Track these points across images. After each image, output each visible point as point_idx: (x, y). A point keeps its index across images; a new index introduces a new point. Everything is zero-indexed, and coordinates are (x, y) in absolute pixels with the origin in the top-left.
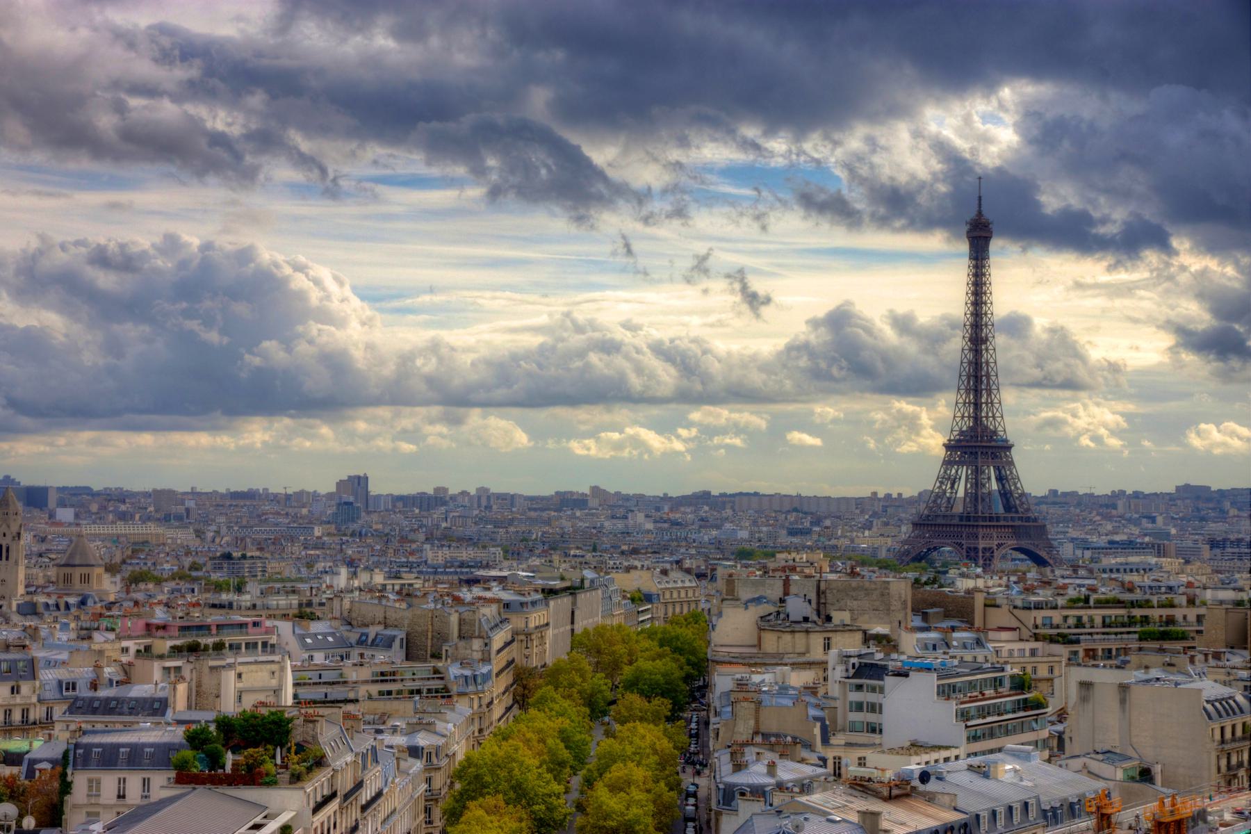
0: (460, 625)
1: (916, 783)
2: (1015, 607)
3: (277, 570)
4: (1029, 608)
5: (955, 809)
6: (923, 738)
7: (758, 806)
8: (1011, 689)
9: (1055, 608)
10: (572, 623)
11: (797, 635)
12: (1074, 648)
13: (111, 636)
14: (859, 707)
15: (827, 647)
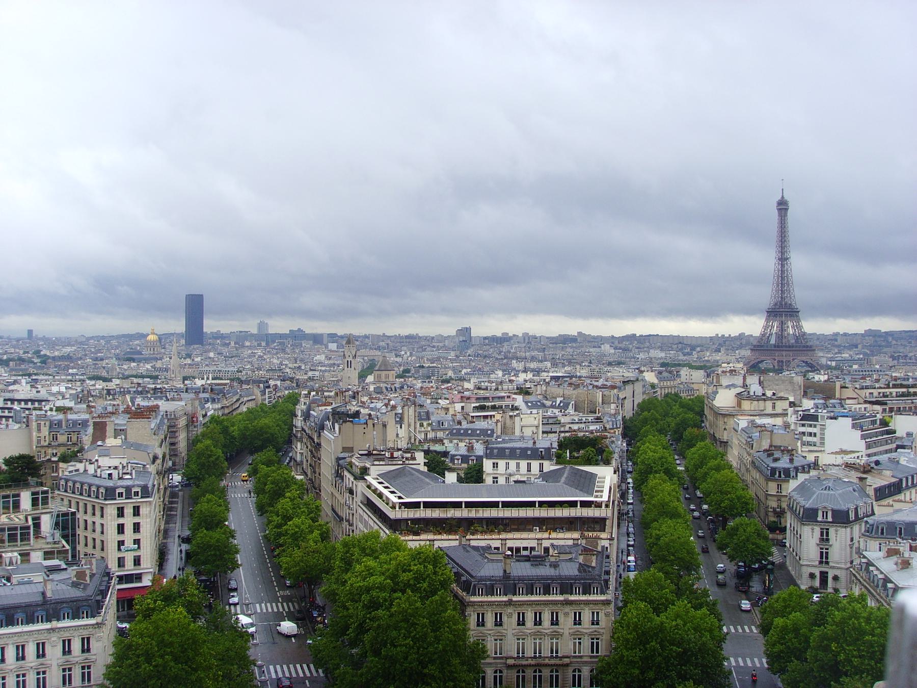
0: (602, 397)
1: (873, 465)
2: (856, 388)
3: (444, 373)
4: (863, 389)
5: (892, 476)
6: (844, 448)
7: (806, 476)
8: (880, 425)
9: (875, 388)
10: (633, 397)
11: (760, 402)
12: (884, 407)
13: (448, 402)
14: (804, 433)
15: (774, 407)
